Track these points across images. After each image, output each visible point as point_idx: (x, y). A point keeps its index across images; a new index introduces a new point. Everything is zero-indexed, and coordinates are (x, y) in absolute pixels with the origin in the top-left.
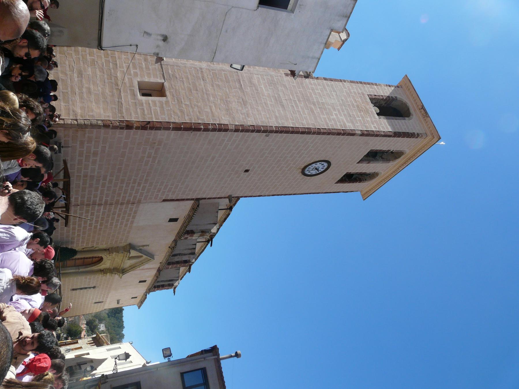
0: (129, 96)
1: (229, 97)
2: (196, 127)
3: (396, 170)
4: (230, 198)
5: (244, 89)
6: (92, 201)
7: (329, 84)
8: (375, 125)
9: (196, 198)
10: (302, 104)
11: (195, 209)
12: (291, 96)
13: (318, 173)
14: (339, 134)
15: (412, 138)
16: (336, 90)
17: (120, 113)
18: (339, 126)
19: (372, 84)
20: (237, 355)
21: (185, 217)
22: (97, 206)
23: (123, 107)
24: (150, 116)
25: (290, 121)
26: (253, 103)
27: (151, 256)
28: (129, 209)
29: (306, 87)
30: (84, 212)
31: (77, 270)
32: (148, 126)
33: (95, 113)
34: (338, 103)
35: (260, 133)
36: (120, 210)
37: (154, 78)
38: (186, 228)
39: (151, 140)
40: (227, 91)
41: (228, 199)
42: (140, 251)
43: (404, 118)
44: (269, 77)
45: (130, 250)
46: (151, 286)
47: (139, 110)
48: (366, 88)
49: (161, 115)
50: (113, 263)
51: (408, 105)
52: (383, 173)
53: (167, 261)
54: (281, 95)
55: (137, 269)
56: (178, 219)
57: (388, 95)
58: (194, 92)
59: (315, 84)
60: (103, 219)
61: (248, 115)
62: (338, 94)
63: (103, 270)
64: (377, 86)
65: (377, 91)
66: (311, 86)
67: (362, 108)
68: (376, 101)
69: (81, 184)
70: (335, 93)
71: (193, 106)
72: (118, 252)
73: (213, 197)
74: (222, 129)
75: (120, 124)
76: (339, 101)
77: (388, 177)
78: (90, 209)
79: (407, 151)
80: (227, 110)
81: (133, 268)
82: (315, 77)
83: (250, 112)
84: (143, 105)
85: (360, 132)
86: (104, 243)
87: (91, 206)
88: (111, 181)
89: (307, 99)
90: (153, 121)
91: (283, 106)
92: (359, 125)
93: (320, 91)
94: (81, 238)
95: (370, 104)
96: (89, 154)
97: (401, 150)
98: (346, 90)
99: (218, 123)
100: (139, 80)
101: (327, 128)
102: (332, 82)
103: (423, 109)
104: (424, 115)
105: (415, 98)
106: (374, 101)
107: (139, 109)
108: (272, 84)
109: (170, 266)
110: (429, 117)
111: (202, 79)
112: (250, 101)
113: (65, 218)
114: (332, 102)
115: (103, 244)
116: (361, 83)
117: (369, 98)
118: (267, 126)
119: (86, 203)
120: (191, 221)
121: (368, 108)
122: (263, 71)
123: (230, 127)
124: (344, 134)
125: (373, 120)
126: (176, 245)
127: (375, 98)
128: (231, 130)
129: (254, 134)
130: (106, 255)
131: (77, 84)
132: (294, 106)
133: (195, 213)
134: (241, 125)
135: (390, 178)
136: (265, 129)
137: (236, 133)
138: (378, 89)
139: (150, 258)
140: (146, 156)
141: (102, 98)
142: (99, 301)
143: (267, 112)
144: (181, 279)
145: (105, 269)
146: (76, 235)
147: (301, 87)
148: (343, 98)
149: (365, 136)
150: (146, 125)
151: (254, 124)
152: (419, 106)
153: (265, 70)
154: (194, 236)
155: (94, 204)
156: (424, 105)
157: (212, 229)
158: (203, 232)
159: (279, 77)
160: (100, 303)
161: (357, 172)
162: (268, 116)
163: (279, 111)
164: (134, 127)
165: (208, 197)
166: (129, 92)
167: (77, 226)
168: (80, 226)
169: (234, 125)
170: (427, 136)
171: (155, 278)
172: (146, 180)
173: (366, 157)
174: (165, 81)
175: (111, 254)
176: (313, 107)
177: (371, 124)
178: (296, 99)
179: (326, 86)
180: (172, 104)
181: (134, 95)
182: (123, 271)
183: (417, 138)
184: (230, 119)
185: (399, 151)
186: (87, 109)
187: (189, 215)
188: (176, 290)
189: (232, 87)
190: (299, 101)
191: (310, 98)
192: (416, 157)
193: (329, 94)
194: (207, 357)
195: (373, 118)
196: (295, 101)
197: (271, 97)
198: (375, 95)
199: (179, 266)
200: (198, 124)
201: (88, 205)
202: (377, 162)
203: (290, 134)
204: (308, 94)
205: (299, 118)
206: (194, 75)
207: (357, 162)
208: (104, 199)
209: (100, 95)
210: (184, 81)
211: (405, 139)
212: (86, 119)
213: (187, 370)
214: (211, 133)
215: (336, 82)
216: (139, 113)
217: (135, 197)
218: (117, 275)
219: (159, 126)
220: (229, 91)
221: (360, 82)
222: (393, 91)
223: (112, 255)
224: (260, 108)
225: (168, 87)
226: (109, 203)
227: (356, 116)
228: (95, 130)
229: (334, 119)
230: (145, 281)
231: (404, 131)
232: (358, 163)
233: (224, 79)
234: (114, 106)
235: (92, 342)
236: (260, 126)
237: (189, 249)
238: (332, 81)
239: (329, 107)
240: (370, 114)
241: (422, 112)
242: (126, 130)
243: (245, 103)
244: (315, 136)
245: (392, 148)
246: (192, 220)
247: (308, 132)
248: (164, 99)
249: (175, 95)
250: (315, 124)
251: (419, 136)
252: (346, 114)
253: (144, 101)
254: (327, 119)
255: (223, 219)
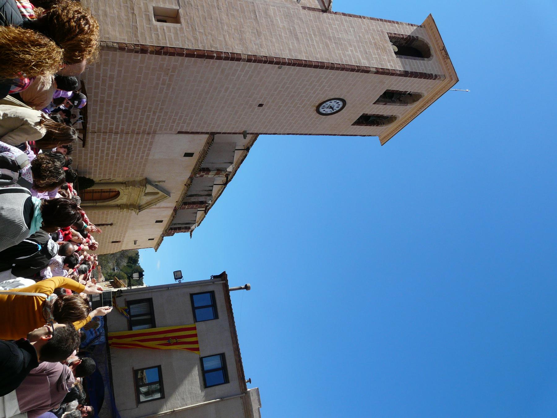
0: (144, 21)
1: (243, 27)
2: (209, 55)
3: (414, 114)
4: (245, 134)
5: (259, 19)
6: (108, 129)
7: (348, 20)
8: (392, 64)
9: (211, 132)
10: (318, 38)
11: (209, 143)
12: (306, 29)
13: (335, 112)
14: (353, 70)
15: (430, 79)
16: (354, 26)
17: (135, 37)
18: (353, 62)
19: (394, 22)
20: (247, 288)
21: (201, 152)
22: (113, 134)
23: (138, 31)
24: (164, 41)
25: (304, 54)
26: (268, 34)
27: (168, 193)
28: (144, 139)
29: (322, 22)
30: (101, 140)
31: (95, 204)
32: (163, 51)
33: (111, 36)
34: (355, 39)
35: (273, 64)
36: (136, 140)
37: (169, 4)
38: (201, 163)
39: (165, 65)
40: (242, 21)
41: (243, 135)
42: (156, 186)
43: (423, 58)
44: (286, 9)
45: (147, 185)
46: (167, 227)
47: (153, 35)
48: (386, 26)
49: (175, 41)
50: (129, 199)
51: (429, 45)
52: (401, 117)
53: (183, 199)
54: (297, 29)
55: (152, 207)
56: (194, 153)
57: (409, 35)
58: (209, 20)
59: (332, 19)
60: (119, 149)
61: (261, 46)
62: (356, 30)
63: (120, 206)
64: (399, 24)
65: (397, 29)
66: (328, 21)
67: (379, 45)
68: (395, 40)
69: (98, 110)
70: (353, 29)
71: (207, 34)
72: (135, 186)
73: (228, 132)
74: (234, 58)
75: (135, 48)
76: (356, 37)
77: (406, 121)
78: (107, 137)
79: (425, 94)
80: (241, 40)
81: (149, 204)
82: (333, 12)
83: (264, 43)
84: (157, 31)
85: (374, 70)
86: (121, 176)
87: (108, 134)
88: (126, 109)
89: (323, 33)
90: (167, 47)
91: (297, 39)
92: (375, 63)
93: (337, 26)
94: (98, 168)
95: (388, 42)
96: (105, 78)
97: (419, 92)
98: (365, 26)
99: (231, 52)
100: (154, 6)
101: (341, 63)
102: (351, 18)
103: (444, 50)
104: (444, 56)
105: (437, 39)
106: (394, 40)
107: (153, 34)
108: (288, 17)
109: (187, 206)
110: (450, 59)
111: (217, 8)
112: (264, 32)
113: (82, 139)
114: (348, 38)
115: (119, 177)
116: (381, 20)
117: (389, 36)
118: (280, 58)
119: (103, 130)
120: (206, 156)
121: (386, 46)
122: (280, 3)
123: (243, 57)
124: (358, 71)
125: (390, 58)
126: (191, 182)
127: (394, 37)
128: (244, 60)
129: (267, 66)
130: (122, 188)
131: (93, 6)
132: (309, 40)
133: (210, 148)
134: (254, 55)
135: (408, 122)
136: (278, 61)
137: (249, 63)
138: (399, 27)
139: (167, 196)
140: (161, 82)
141: (118, 22)
142: (115, 243)
143: (280, 44)
144: (199, 225)
145: (122, 204)
146: (93, 165)
147: (317, 21)
148: (361, 35)
149: (380, 74)
150: (160, 50)
151: (267, 55)
152: (440, 47)
153: (282, 2)
154: (210, 174)
155: (111, 131)
156: (445, 46)
157: (228, 168)
158: (219, 171)
159: (296, 10)
160: (117, 243)
161: (373, 113)
162: (282, 48)
163: (293, 43)
164: (149, 51)
165: (223, 132)
166: (144, 16)
167: (94, 155)
168: (97, 155)
169: (247, 55)
170: (445, 78)
171: (172, 218)
172: (161, 109)
173: (383, 98)
174: (180, 8)
175: (128, 187)
176: (328, 42)
177: (388, 63)
178: (311, 33)
179: (344, 21)
180: (186, 30)
181: (149, 20)
182: (140, 208)
183: (434, 79)
184: (243, 49)
185: (417, 93)
186: (103, 31)
187: (204, 150)
188: (193, 233)
189: (247, 17)
190: (315, 35)
191: (326, 33)
192: (433, 101)
193: (347, 29)
194: (215, 282)
195: (390, 57)
196: (310, 35)
197: (287, 30)
198: (395, 34)
199: (196, 207)
200: (211, 52)
201: (105, 133)
202: (394, 104)
203: (303, 67)
204: (325, 28)
205: (313, 52)
206: (209, 3)
207: (373, 103)
208: (120, 127)
209: (116, 18)
210: (199, 8)
211: (423, 80)
212: (102, 40)
213: (196, 292)
214: (224, 62)
215: (355, 18)
216: (154, 38)
217: (151, 127)
218: (133, 211)
219: (172, 51)
220: (244, 21)
221: (380, 19)
222: (415, 30)
223: (128, 189)
224: (274, 40)
225: (182, 13)
226: (125, 132)
227: (372, 54)
228: (111, 53)
229: (349, 55)
230: (161, 221)
231: (422, 72)
232: (374, 104)
233: (240, 9)
234: (129, 30)
235: (110, 285)
236: (273, 58)
237: (206, 191)
238: (351, 16)
239: (346, 43)
240: (387, 52)
241: (443, 54)
242: (141, 54)
243: (259, 34)
244: (328, 70)
245: (409, 90)
246: (207, 155)
247: (321, 66)
248: (178, 26)
249: (189, 22)
250: (329, 58)
251: (437, 77)
252: (362, 50)
253: (158, 27)
254: (342, 54)
255: (240, 161)
